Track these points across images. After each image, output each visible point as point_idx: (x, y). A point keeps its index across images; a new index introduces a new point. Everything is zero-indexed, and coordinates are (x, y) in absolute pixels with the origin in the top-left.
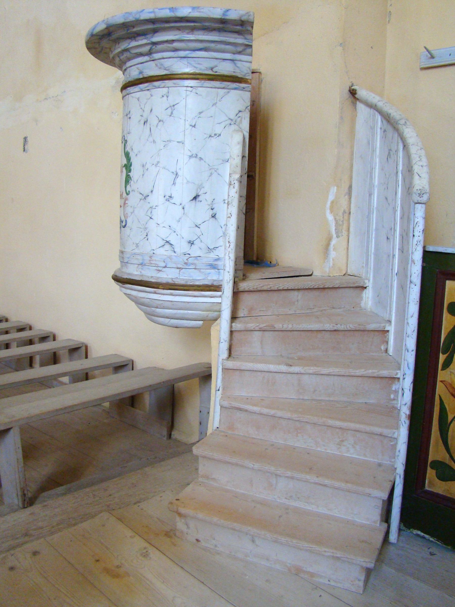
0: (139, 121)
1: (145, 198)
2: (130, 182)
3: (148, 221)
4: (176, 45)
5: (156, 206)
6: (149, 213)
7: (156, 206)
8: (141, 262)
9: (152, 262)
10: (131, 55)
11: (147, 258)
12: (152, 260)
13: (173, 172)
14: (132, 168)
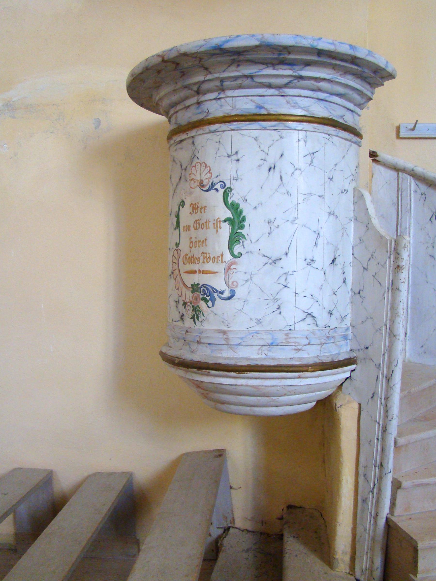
0: (260, 166)
4: (323, 85)
6: (282, 280)
8: (270, 342)
9: (289, 340)
11: (281, 337)
12: (290, 338)
13: (315, 232)
14: (246, 224)
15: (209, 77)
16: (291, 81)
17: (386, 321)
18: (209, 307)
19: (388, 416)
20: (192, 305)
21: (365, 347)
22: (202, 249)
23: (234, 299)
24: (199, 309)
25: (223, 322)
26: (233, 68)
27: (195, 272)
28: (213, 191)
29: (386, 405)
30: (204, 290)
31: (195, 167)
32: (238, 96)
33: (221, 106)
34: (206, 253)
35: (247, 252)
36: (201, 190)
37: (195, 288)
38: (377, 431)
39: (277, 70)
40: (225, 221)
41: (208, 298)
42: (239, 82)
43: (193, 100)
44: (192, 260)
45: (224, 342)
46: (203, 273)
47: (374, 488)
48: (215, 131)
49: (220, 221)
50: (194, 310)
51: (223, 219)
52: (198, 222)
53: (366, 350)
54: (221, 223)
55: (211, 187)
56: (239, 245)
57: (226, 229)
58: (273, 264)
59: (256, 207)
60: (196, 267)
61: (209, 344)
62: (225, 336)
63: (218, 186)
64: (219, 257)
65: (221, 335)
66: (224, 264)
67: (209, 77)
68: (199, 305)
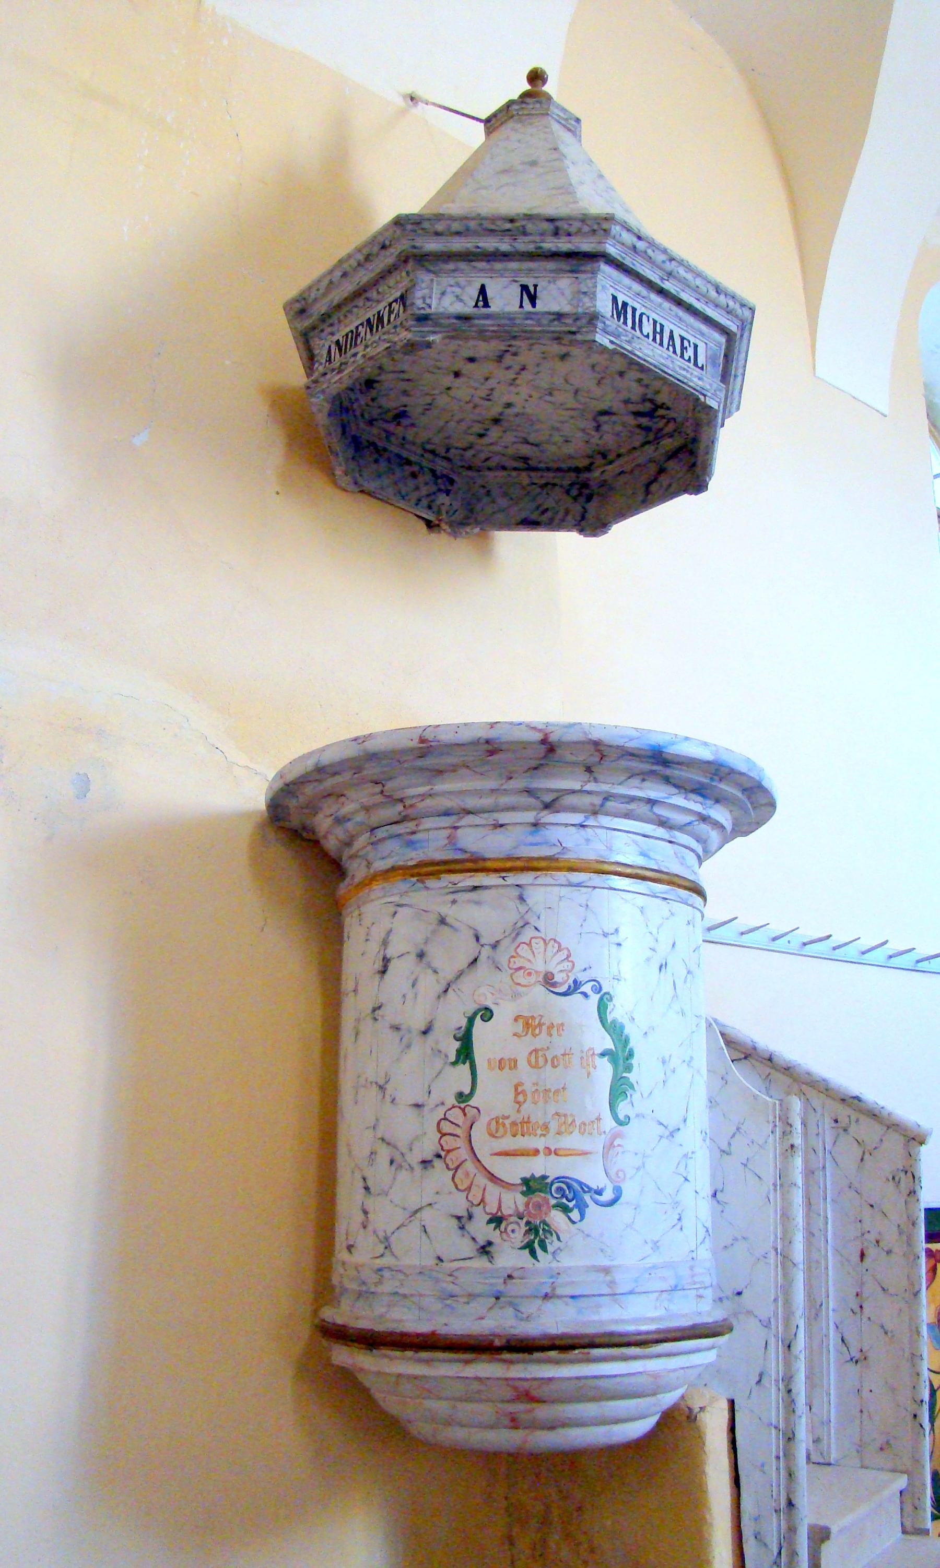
0: (648, 960)
1: (672, 1135)
2: (631, 1095)
3: (681, 1185)
5: (693, 1153)
6: (681, 1169)
7: (693, 1153)
8: (672, 1282)
9: (696, 1279)
10: (650, 814)
14: (634, 1061)
15: (590, 787)
16: (693, 821)
17: (775, 1241)
18: (574, 1222)
19: (796, 1409)
20: (525, 1220)
21: (736, 1292)
22: (552, 1108)
23: (622, 1204)
24: (547, 1228)
25: (602, 1250)
26: (636, 781)
27: (536, 1152)
28: (577, 997)
29: (789, 1391)
30: (559, 1189)
31: (529, 944)
32: (615, 830)
33: (588, 840)
34: (565, 1116)
35: (637, 1116)
36: (548, 992)
37: (531, 1185)
38: (774, 1441)
39: (688, 800)
40: (603, 1055)
41: (571, 1204)
42: (632, 806)
43: (530, 817)
44: (522, 1127)
45: (606, 1290)
46: (556, 1154)
47: (780, 1553)
48: (578, 885)
49: (593, 1054)
50: (532, 1229)
51: (599, 1051)
52: (540, 1053)
53: (737, 1298)
54: (597, 1057)
55: (572, 988)
56: (625, 1102)
57: (605, 1071)
58: (670, 1138)
59: (646, 1033)
60: (539, 1143)
61: (573, 1297)
62: (608, 1278)
63: (587, 988)
64: (592, 1122)
65: (601, 1277)
66: (603, 1136)
67: (590, 787)
68: (546, 1219)
